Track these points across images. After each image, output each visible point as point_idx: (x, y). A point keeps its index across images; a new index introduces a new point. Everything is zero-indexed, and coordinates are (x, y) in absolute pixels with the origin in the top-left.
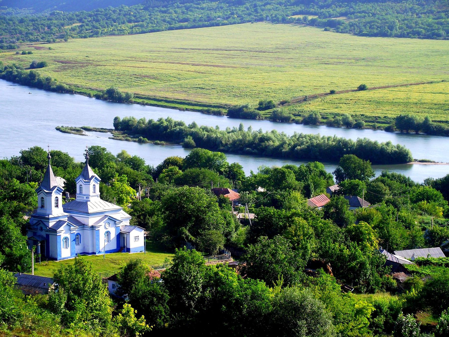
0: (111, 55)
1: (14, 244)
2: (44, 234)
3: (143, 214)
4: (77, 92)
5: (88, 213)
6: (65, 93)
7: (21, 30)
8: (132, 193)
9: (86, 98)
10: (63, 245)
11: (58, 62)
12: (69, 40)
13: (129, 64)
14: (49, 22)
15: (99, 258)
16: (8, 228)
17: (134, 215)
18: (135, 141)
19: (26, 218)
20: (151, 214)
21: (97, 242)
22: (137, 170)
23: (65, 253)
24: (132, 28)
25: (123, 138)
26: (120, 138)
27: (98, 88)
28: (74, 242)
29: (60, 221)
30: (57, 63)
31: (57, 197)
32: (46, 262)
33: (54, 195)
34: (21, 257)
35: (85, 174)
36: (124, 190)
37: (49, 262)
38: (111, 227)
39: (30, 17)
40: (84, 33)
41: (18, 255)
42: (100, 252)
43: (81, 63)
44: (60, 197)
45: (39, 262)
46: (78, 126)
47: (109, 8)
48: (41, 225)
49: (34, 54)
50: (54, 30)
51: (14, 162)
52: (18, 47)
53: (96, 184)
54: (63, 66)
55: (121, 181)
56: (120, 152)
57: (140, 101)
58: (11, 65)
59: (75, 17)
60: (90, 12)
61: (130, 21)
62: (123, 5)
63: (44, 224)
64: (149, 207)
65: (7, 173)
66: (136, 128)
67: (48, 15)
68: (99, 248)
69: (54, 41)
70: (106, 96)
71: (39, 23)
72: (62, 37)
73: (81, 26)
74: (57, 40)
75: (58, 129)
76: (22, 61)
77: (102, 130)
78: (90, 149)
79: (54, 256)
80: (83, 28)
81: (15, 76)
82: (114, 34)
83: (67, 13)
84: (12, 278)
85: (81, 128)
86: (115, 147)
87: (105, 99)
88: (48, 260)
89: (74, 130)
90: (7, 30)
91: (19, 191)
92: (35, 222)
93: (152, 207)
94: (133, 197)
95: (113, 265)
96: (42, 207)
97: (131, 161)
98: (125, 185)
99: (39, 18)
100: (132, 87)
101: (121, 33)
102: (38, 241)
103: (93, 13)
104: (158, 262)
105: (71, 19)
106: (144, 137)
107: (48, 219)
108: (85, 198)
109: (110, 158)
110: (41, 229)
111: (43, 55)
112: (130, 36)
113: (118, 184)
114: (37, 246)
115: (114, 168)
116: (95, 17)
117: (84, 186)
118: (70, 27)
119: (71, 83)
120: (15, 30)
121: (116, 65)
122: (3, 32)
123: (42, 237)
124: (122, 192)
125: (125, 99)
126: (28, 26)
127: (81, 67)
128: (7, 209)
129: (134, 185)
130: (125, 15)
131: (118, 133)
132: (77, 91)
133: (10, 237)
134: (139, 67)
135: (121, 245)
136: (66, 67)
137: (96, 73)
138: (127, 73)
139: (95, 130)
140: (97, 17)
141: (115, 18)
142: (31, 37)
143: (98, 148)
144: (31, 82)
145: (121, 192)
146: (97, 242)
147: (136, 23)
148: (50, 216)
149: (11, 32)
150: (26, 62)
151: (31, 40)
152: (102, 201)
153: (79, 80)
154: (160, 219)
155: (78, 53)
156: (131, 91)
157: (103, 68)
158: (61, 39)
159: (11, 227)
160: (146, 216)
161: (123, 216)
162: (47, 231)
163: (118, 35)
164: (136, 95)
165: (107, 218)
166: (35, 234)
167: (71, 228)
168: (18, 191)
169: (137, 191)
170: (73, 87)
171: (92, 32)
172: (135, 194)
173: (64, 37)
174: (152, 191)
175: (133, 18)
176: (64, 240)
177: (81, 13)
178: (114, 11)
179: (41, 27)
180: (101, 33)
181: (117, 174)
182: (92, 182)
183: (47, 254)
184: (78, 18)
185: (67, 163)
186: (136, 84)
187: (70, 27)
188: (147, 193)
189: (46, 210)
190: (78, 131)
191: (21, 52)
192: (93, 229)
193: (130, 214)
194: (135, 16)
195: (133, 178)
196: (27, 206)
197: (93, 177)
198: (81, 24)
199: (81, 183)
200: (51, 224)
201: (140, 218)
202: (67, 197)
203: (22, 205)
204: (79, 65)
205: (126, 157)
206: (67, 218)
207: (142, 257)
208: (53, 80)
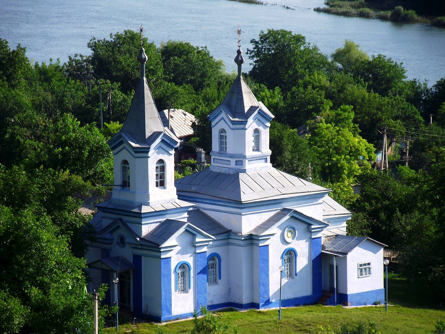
1: (51, 280)
2: (127, 253)
3: (386, 208)
5: (240, 202)
8: (365, 153)
10: (176, 284)
15: (266, 318)
16: (38, 239)
17: (363, 209)
18: (383, 18)
19: (85, 212)
20: (407, 206)
21: (263, 276)
22: (383, 93)
25: (353, 11)
26: (344, 10)
28: (205, 276)
29: (168, 221)
34: (69, 312)
35: (234, 102)
36: (343, 143)
37: (140, 325)
38: (298, 239)
41: (62, 308)
42: (268, 303)
44: (170, 161)
45: (113, 325)
48: (122, 231)
53: (261, 128)
55: (338, 121)
56: (341, 46)
63: (130, 230)
64: (401, 190)
65: (50, 97)
68: (267, 291)
78: (264, 38)
79: (153, 311)
91: (78, 145)
92: (106, 223)
93: (411, 189)
94: (366, 162)
96: (125, 184)
97: (369, 70)
98: (347, 132)
102: (113, 271)
109: (314, 61)
110: (122, 241)
113: (327, 129)
114: (111, 285)
117: (230, 134)
123: (124, 261)
124: (338, 151)
128: (35, 189)
129: (371, 131)
133: (42, 260)
143: (283, 36)
145: (335, 149)
146: (263, 276)
148: (145, 209)
152: (275, 172)
154: (427, 220)
159: (45, 235)
160: (394, 212)
161: (328, 211)
162: (136, 246)
165: (287, 217)
166: (106, 253)
167: (198, 240)
168: (71, 145)
169: (379, 148)
172: (373, 155)
174: (418, 147)
176: (179, 271)
182: (252, 124)
185: (203, 75)
188: (405, 154)
189: (134, 193)
192: (252, 244)
193: (352, 207)
196: (89, 184)
197: (253, 109)
199: (222, 125)
200: (147, 229)
201: (378, 218)
202: (200, 162)
203: (78, 179)
205: (357, 60)
206: (186, 215)
207: (376, 318)
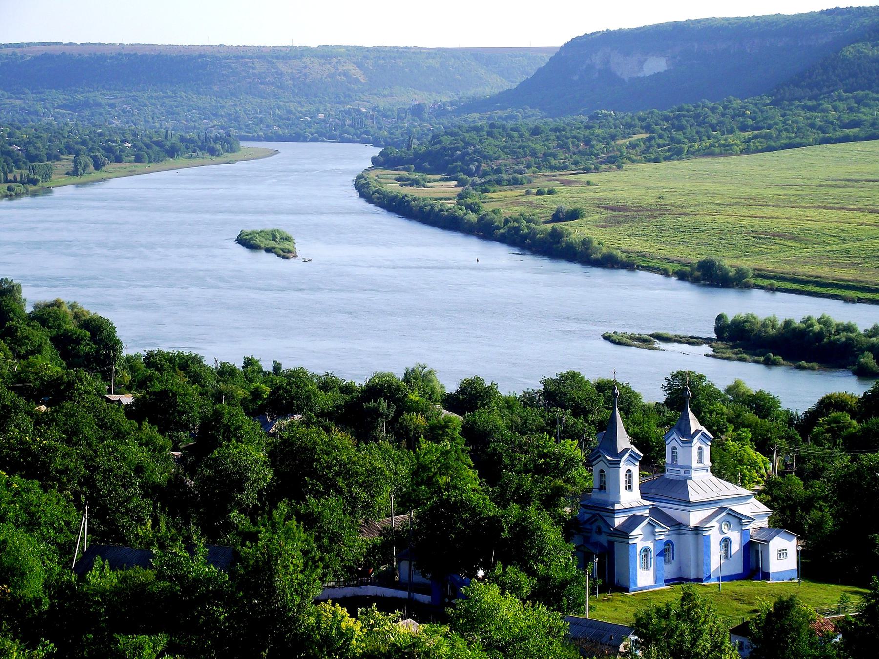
0: (707, 193)
2: (603, 539)
4: (642, 267)
5: (689, 502)
6: (618, 268)
7: (534, 149)
8: (761, 465)
9: (659, 278)
10: (641, 563)
11: (605, 208)
12: (625, 167)
13: (742, 210)
14: (587, 133)
15: (709, 590)
16: (539, 528)
21: (706, 558)
23: (644, 578)
24: (748, 141)
25: (734, 356)
27: (682, 259)
30: (602, 210)
31: (629, 470)
40: (655, 151)
43: (649, 210)
44: (635, 470)
46: (645, 332)
47: (702, 102)
48: (600, 523)
49: (559, 194)
50: (597, 147)
52: (530, 181)
54: (614, 216)
55: (738, 439)
56: (731, 383)
57: (766, 283)
58: (516, 216)
59: (637, 122)
60: (665, 112)
61: (743, 129)
62: (731, 98)
66: (758, 337)
67: (585, 118)
69: (597, 170)
71: (569, 134)
72: (612, 160)
73: (649, 139)
74: (603, 166)
75: (607, 338)
76: (536, 207)
77: (693, 341)
78: (674, 377)
80: (653, 142)
81: (525, 237)
82: (712, 154)
83: (622, 115)
85: (651, 336)
86: (724, 373)
87: (695, 281)
88: (613, 591)
89: (638, 339)
90: (509, 148)
92: (587, 516)
95: (736, 604)
96: (602, 488)
97: (752, 401)
98: (747, 448)
99: (568, 124)
100: (750, 256)
101: (727, 150)
103: (671, 114)
104: (826, 602)
105: (629, 126)
106: (775, 355)
107: (613, 511)
108: (682, 473)
109: (713, 395)
110: (599, 531)
111: (576, 195)
112: (744, 157)
115: (723, 414)
116: (676, 122)
117: (679, 450)
118: (627, 141)
119: (630, 248)
120: (523, 148)
121: (718, 213)
122: (501, 153)
123: (601, 546)
124: (741, 462)
125: (735, 279)
126: (548, 140)
127: (649, 217)
129: (764, 446)
130: (733, 117)
132: (642, 263)
134: (762, 217)
135: (752, 563)
136: (621, 219)
137: (678, 230)
138: (738, 229)
139: (679, 340)
140: (680, 121)
141: (714, 121)
142: (553, 162)
144: (552, 247)
146: (706, 558)
147: (756, 132)
148: (617, 507)
149: (515, 152)
150: (544, 210)
151: (553, 168)
152: (714, 478)
153: (645, 244)
155: (643, 192)
156: (747, 264)
157: (692, 219)
158: (610, 165)
159: (545, 526)
161: (754, 509)
162: (610, 534)
163: (721, 154)
164: (757, 272)
165: (724, 514)
166: (586, 540)
170: (634, 257)
171: (669, 150)
173: (615, 161)
174: (800, 460)
175: (750, 122)
176: (643, 554)
177: (649, 113)
178: (713, 110)
179: (573, 143)
180: (688, 152)
181: (731, 427)
183: (612, 582)
184: (644, 124)
186: (757, 250)
187: (627, 141)
189: (608, 494)
190: (644, 341)
191: (535, 191)
192: (697, 534)
194: (753, 119)
195: (760, 435)
198: (648, 135)
199: (674, 443)
200: (618, 521)
204: (646, 213)
205: (744, 394)
206: (647, 511)
208: (595, 243)
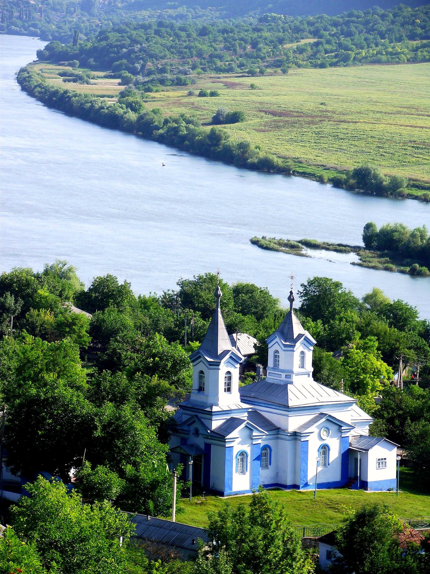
0: (370, 101)
1: (142, 460)
2: (200, 442)
3: (399, 416)
4: (298, 172)
5: (288, 407)
6: (274, 173)
7: (201, 50)
8: (385, 374)
9: (315, 184)
10: (237, 467)
11: (266, 112)
12: (290, 71)
13: (403, 120)
14: (255, 35)
15: (304, 497)
16: (133, 428)
17: (382, 417)
18: (403, 272)
19: (170, 409)
22: (401, 329)
23: (240, 482)
24: (415, 50)
25: (380, 266)
27: (338, 167)
28: (259, 462)
29: (232, 419)
30: (263, 114)
31: (229, 373)
32: (202, 499)
33: (224, 368)
35: (286, 331)
37: (208, 497)
38: (331, 437)
39: (221, 24)
40: (322, 57)
42: (306, 485)
43: (310, 116)
44: (236, 372)
45: (188, 496)
46: (294, 238)
47: (373, 9)
48: (197, 425)
49: (221, 97)
50: (264, 51)
51: (168, 302)
52: (193, 82)
53: (306, 351)
54: (274, 121)
55: (365, 348)
56: (370, 292)
57: (420, 193)
59: (306, 26)
60: (335, 18)
61: (412, 37)
62: (402, 5)
64: (412, 403)
66: (407, 246)
67: (255, 21)
68: (306, 476)
69: (262, 73)
70: (352, 181)
71: (236, 36)
72: (278, 64)
73: (317, 44)
74: (269, 70)
75: (255, 242)
76: (197, 108)
77: (341, 249)
78: (311, 283)
79: (219, 487)
80: (320, 47)
81: (184, 138)
82: (379, 62)
83: (292, 19)
84: (127, 525)
85: (299, 242)
86: (357, 280)
87: (350, 189)
88: (207, 494)
89: (286, 245)
90: (175, 48)
92: (185, 418)
93: (419, 403)
94: (385, 380)
95: (330, 513)
96: (201, 389)
98: (372, 357)
99: (237, 26)
100: (406, 166)
101: (394, 58)
102: (189, 455)
103: (340, 20)
104: (421, 513)
105: (297, 30)
106: (421, 265)
107: (211, 413)
108: (283, 377)
109: (348, 302)
110: (197, 433)
111: (238, 98)
112: (411, 66)
113: (357, 355)
115: (353, 322)
116: (345, 28)
117: (282, 354)
118: (294, 45)
119: (287, 154)
120: (189, 48)
121: (378, 121)
122: (167, 53)
123: (197, 448)
124: (364, 371)
125: (390, 189)
126: (215, 41)
127: (309, 123)
128: (133, 390)
129: (390, 357)
131: (370, 255)
132: (298, 169)
133: (135, 444)
134: (422, 127)
136: (281, 124)
137: (336, 137)
138: (397, 138)
139: (327, 247)
140: (349, 27)
141: (383, 29)
142: (219, 63)
143: (326, 282)
144: (210, 149)
145: (363, 369)
146: (304, 464)
147: (425, 41)
148: (215, 409)
149: (181, 52)
150: (205, 112)
151: (218, 70)
153: (303, 150)
155: (306, 97)
156: (403, 173)
157: (352, 126)
158: (275, 69)
159: (139, 426)
160: (405, 419)
161: (356, 417)
162: (207, 437)
163: (387, 62)
164: (412, 182)
165: (324, 420)
166: (184, 441)
167: (254, 434)
169: (396, 370)
170: (290, 163)
171: (336, 56)
172: (391, 375)
173: (281, 65)
175: (419, 31)
176: (239, 457)
177: (318, 18)
178: (383, 17)
179: (240, 45)
180: (355, 59)
181: (358, 335)
182: (299, 347)
183: (204, 482)
184: (312, 29)
185: (264, 309)
186: (414, 159)
187: (294, 45)
189: (207, 396)
190: (292, 247)
191: (197, 92)
192: (296, 439)
194: (423, 27)
195: (389, 344)
196: (173, 387)
197: (300, 336)
198: (316, 40)
199: (276, 347)
200: (216, 424)
202: (259, 375)
203: (165, 384)
204: (307, 119)
205: (381, 303)
206: (246, 414)
207: (389, 501)
208: (252, 147)
